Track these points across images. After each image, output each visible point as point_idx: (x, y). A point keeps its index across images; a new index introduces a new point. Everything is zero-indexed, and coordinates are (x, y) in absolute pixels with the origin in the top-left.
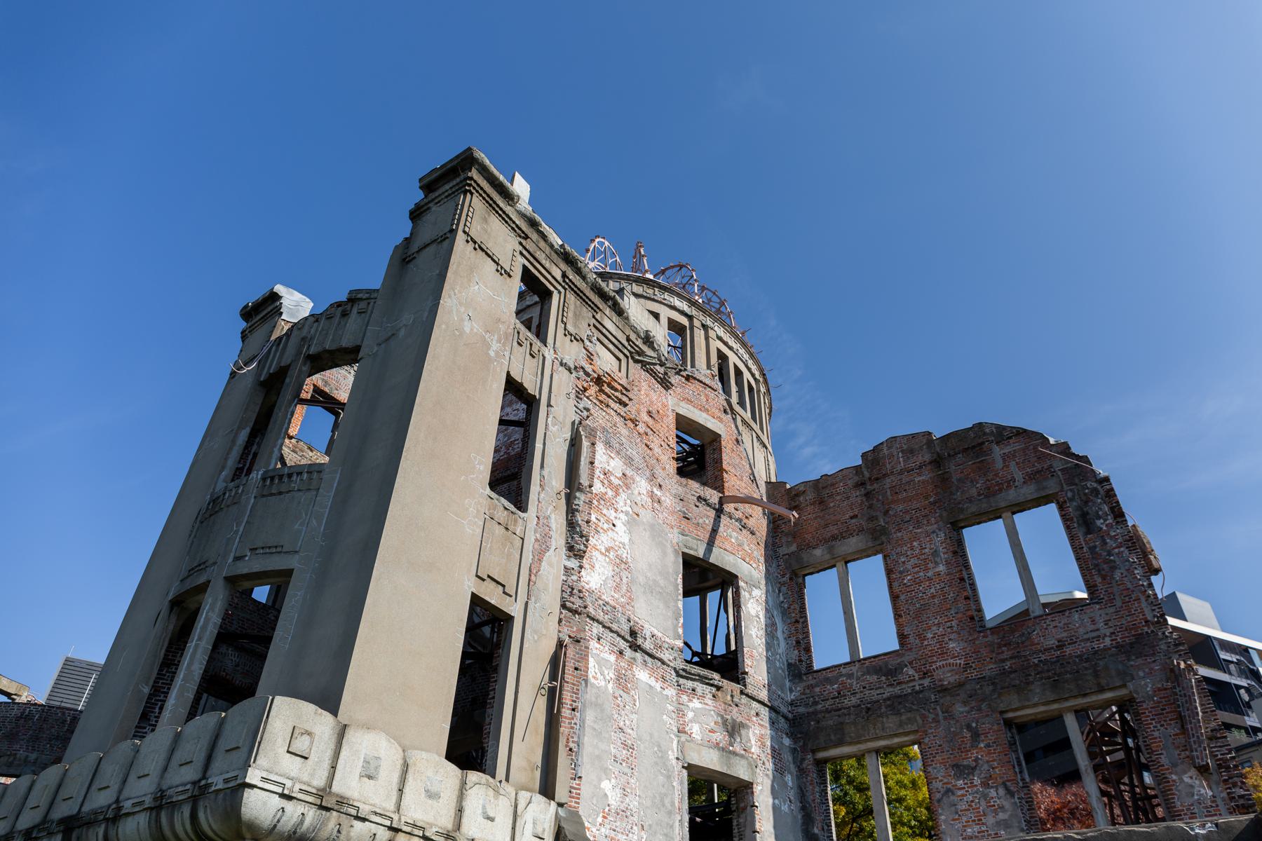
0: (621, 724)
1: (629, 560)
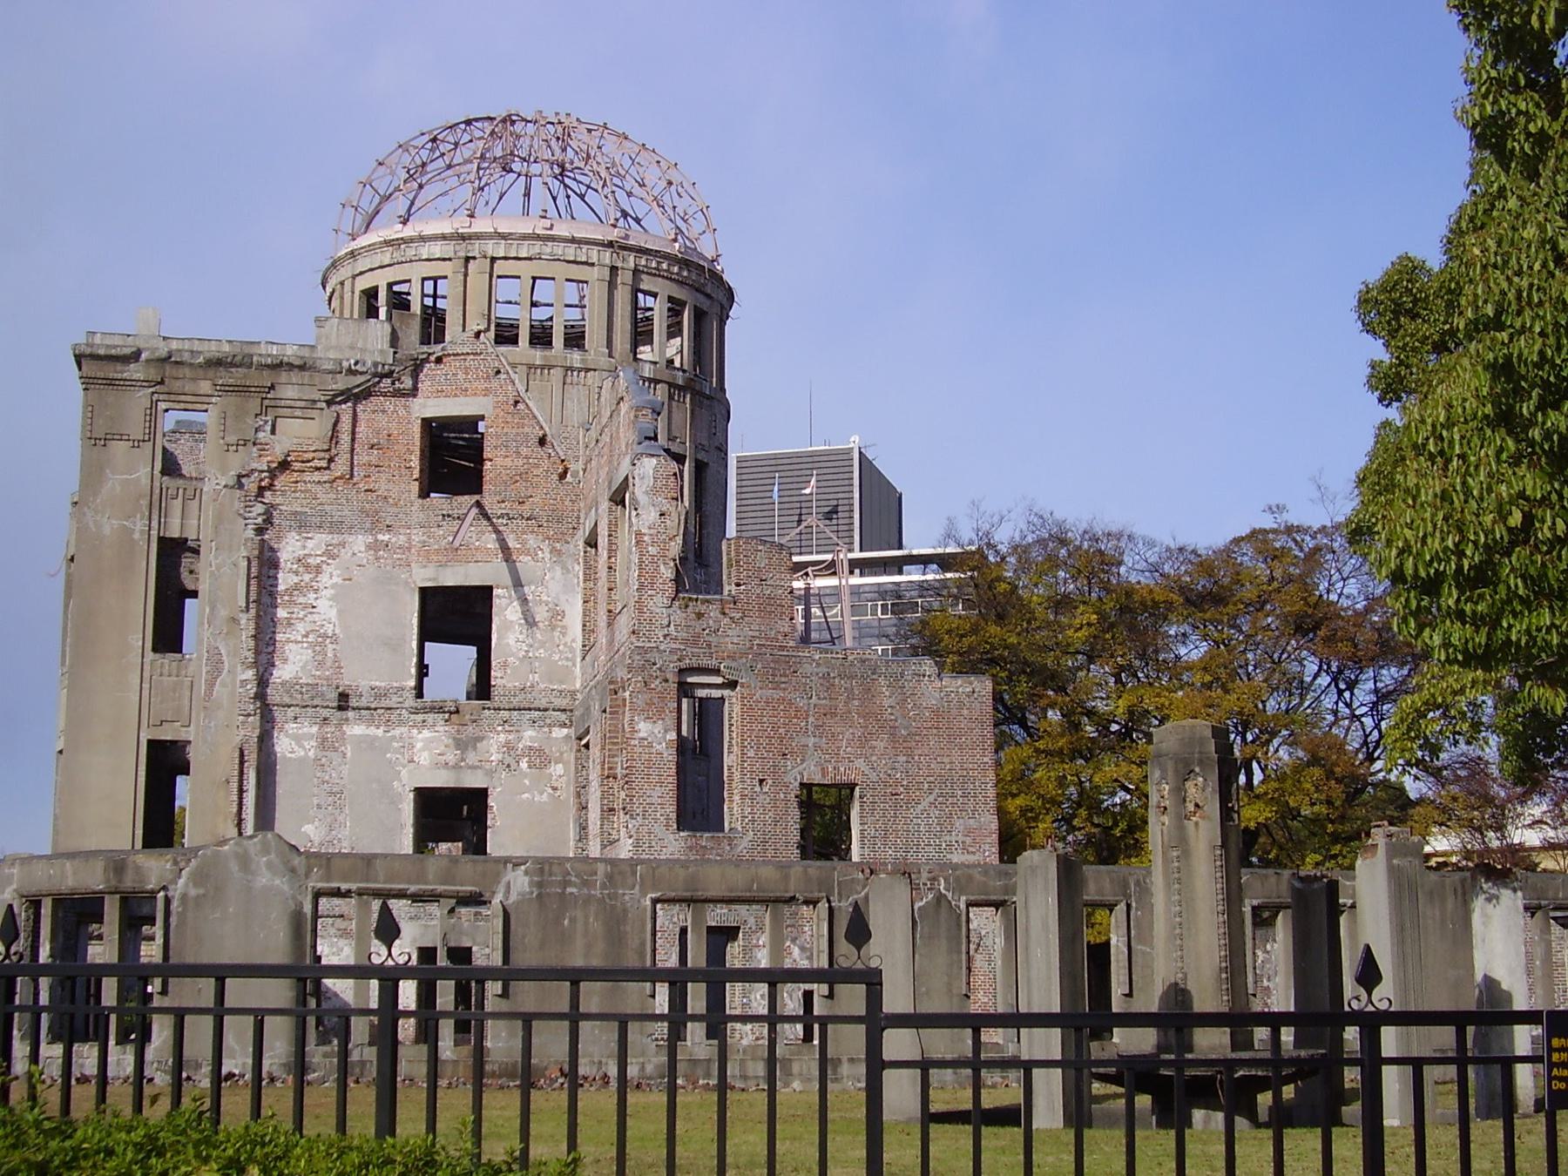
0: (327, 778)
1: (337, 632)
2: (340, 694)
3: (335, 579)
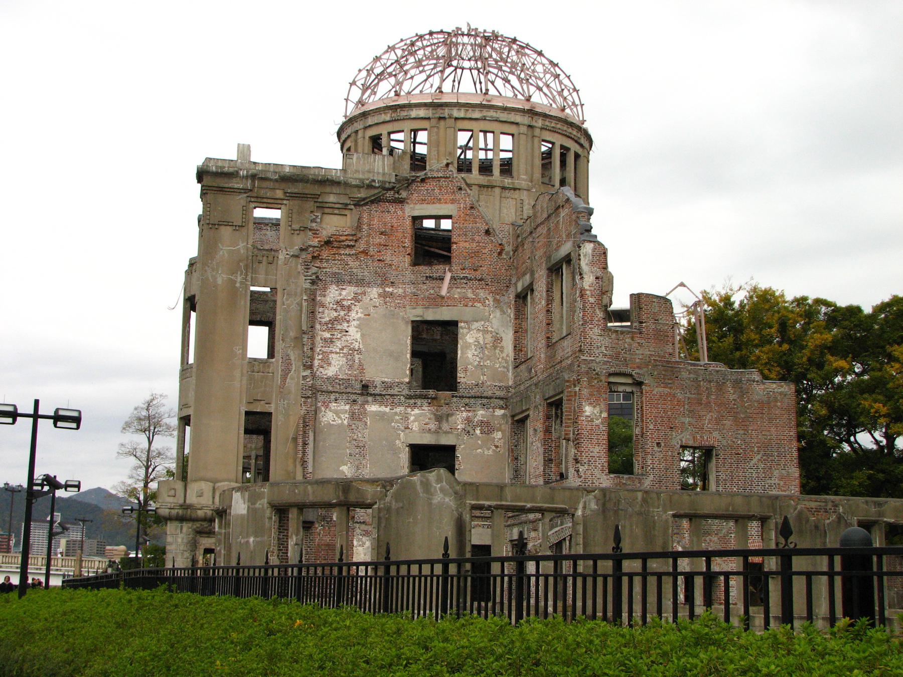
1: (361, 347)
2: (363, 386)
3: (360, 315)
